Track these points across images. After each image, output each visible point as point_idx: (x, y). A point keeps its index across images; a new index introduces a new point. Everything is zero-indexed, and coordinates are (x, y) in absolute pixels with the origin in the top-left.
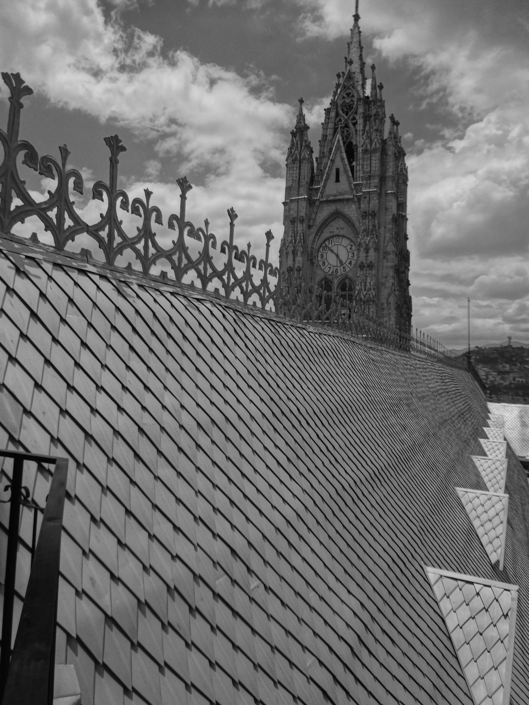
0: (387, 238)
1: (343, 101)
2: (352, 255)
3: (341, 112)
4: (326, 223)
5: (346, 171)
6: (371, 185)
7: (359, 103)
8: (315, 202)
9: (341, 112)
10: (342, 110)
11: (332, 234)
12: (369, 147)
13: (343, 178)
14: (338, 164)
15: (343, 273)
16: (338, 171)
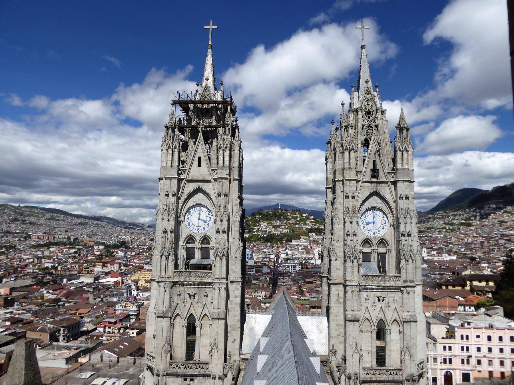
0: (235, 211)
5: (206, 160)
6: (224, 173)
8: (183, 180)
11: (195, 203)
12: (222, 145)
14: (200, 153)
15: (203, 231)
16: (200, 158)
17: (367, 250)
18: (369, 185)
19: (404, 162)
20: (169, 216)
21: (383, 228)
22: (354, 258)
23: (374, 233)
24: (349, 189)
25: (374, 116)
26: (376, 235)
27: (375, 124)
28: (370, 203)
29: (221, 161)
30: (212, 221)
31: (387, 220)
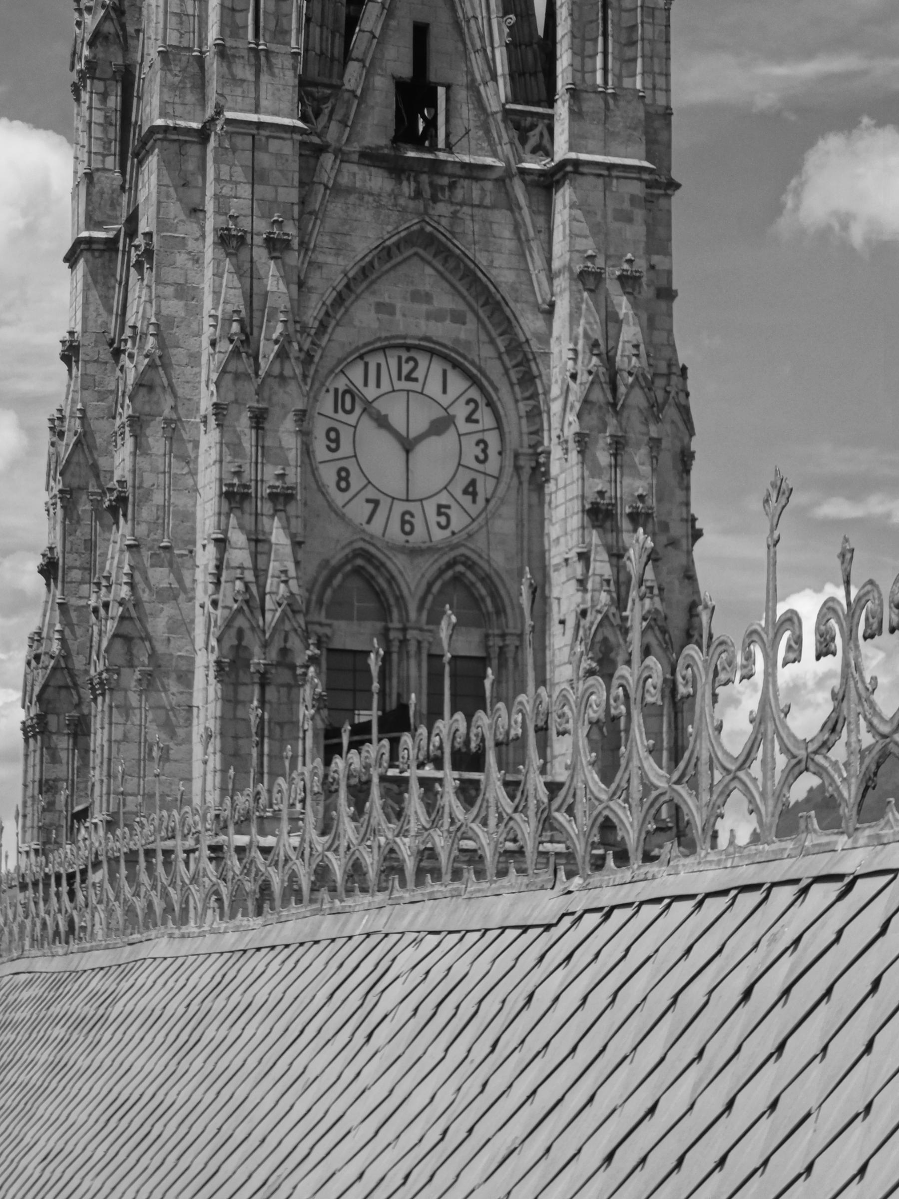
18: (378, 181)
21: (471, 490)
22: (273, 655)
23: (406, 520)
24: (245, 190)
26: (418, 537)
28: (385, 308)
31: (492, 439)
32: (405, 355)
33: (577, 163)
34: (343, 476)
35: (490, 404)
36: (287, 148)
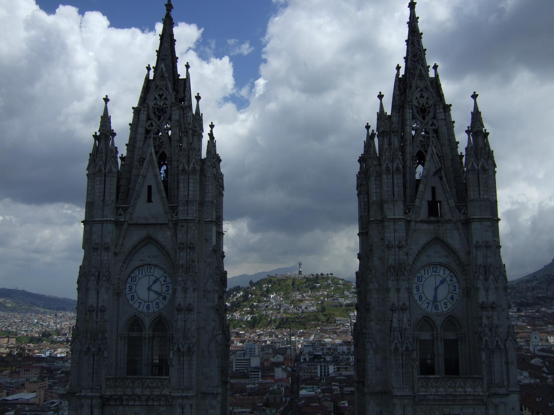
1: (154, 102)
2: (166, 289)
3: (152, 115)
4: (135, 249)
7: (173, 108)
9: (152, 115)
10: (154, 112)
12: (187, 168)
13: (155, 197)
15: (156, 310)
16: (150, 188)
17: (426, 336)
18: (425, 226)
19: (481, 188)
20: (98, 283)
21: (452, 298)
22: (404, 348)
25: (431, 115)
26: (440, 310)
27: (433, 127)
29: (182, 192)
30: (171, 292)
31: (457, 285)
32: (434, 266)
33: (473, 219)
34: (420, 297)
35: (455, 276)
36: (402, 224)
